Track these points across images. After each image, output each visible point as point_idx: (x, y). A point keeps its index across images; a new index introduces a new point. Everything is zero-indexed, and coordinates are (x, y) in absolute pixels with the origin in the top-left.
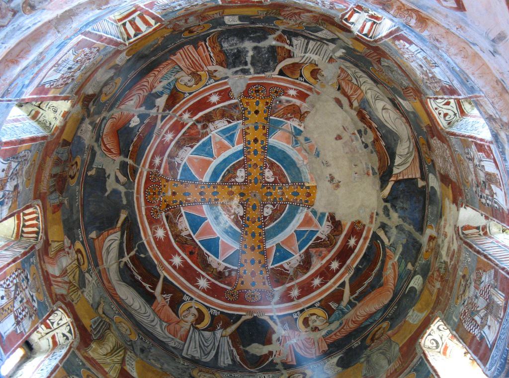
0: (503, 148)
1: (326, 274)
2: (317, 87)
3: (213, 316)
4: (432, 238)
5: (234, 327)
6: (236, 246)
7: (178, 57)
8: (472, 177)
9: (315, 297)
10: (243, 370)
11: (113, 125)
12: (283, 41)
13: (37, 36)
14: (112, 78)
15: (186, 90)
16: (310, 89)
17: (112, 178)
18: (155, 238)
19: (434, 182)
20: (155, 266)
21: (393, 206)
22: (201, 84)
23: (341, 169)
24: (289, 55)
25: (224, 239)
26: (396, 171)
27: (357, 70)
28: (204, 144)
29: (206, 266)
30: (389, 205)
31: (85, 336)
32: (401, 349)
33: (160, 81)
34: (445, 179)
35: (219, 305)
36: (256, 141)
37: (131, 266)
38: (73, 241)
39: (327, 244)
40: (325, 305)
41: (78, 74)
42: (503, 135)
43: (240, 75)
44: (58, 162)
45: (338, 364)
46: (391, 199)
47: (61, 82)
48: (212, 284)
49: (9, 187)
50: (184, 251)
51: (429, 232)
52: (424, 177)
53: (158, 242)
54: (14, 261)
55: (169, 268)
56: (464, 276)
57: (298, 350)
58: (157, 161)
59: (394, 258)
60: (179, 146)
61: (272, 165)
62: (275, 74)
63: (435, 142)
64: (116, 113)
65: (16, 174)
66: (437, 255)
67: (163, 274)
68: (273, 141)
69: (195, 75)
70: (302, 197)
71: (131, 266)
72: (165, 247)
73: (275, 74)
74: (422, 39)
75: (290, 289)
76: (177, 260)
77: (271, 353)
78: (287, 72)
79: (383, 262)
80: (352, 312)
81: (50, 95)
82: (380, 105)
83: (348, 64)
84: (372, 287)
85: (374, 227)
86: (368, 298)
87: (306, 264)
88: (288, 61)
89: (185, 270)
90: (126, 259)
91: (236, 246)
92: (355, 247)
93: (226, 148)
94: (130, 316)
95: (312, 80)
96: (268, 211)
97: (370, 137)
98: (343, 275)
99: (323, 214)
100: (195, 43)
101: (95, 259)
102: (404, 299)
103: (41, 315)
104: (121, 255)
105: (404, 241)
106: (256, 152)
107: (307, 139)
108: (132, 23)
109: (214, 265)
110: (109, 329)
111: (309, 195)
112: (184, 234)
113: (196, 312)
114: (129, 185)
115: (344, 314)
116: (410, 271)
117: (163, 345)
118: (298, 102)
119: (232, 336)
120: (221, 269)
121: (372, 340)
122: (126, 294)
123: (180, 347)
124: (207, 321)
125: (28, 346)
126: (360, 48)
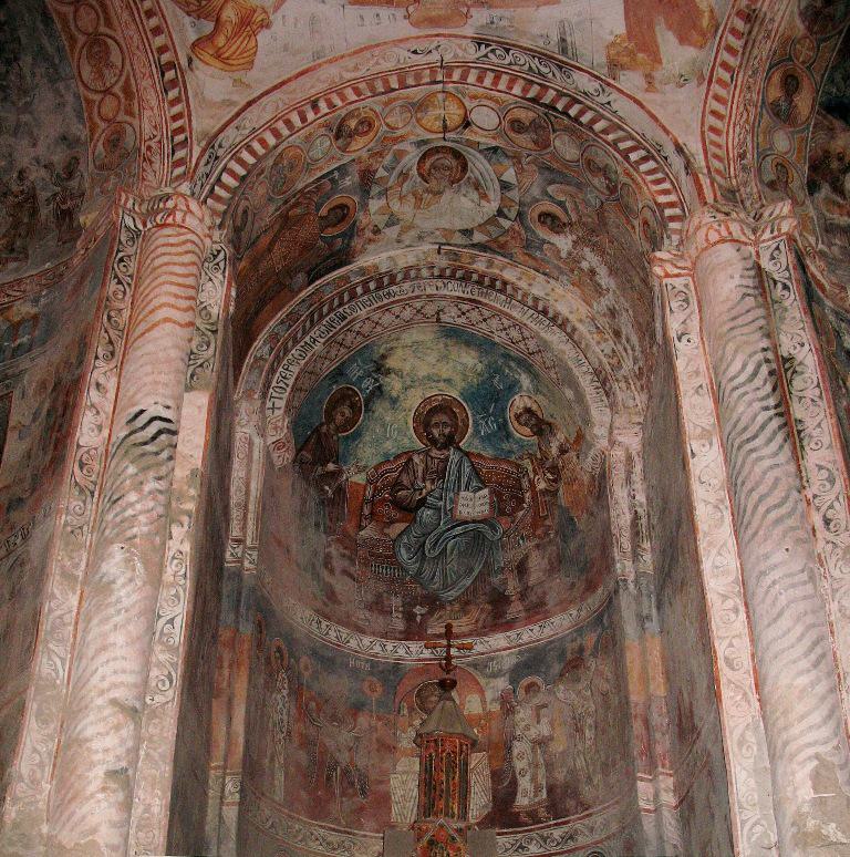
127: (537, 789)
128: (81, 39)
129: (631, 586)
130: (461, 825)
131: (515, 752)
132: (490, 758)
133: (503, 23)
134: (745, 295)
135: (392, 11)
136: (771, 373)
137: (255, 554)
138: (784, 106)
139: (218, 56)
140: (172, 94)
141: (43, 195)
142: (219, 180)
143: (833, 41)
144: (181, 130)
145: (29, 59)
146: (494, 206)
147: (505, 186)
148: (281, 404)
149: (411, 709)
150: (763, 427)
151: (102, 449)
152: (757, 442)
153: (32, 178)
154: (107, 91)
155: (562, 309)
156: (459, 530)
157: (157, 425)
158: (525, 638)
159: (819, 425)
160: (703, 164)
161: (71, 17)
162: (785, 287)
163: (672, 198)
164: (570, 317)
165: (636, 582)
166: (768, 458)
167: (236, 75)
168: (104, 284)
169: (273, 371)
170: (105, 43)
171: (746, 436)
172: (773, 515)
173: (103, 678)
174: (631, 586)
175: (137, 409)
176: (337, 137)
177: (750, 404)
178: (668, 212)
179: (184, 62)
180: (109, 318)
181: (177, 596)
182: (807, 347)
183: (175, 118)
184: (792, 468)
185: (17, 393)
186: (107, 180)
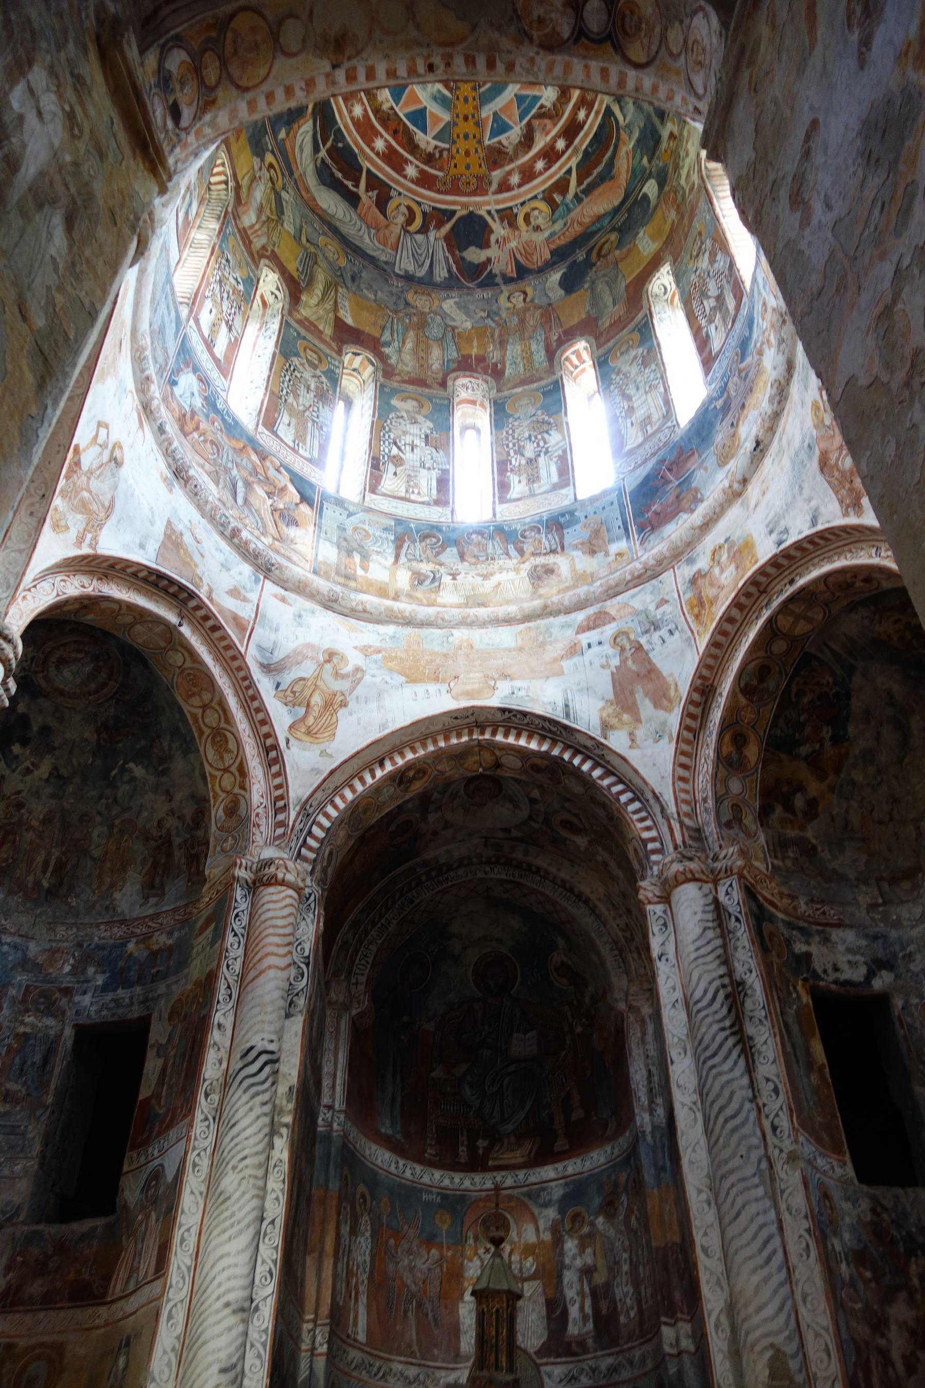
1: (550, 155)
3: (424, 214)
5: (448, 227)
6: (446, 117)
10: (461, 287)
18: (352, 119)
20: (355, 156)
25: (434, 109)
29: (413, 147)
31: (295, 289)
32: (627, 287)
35: (431, 199)
37: (329, 161)
39: (551, 115)
48: (422, 172)
50: (387, 130)
53: (356, 123)
55: (370, 159)
57: (518, 256)
59: (628, 145)
67: (366, 164)
71: (329, 161)
72: (366, 130)
75: (509, 173)
76: (380, 144)
77: (489, 260)
80: (578, 209)
86: (596, 193)
89: (392, 159)
90: (323, 153)
91: (446, 117)
92: (585, 122)
94: (335, 231)
98: (569, 159)
101: (288, 166)
104: (316, 149)
105: (642, 124)
109: (423, 145)
110: (316, 263)
112: (385, 107)
113: (406, 211)
115: (569, 210)
116: (644, 170)
117: (373, 260)
119: (447, 238)
120: (430, 149)
122: (329, 201)
123: (391, 260)
124: (418, 221)
127: (585, 1318)
129: (649, 1138)
130: (509, 1378)
131: (566, 1281)
132: (545, 1286)
133: (522, 693)
134: (705, 929)
135: (438, 686)
136: (727, 997)
137: (342, 1116)
138: (735, 757)
139: (309, 733)
141: (177, 841)
142: (310, 833)
144: (281, 797)
145: (168, 737)
146: (524, 813)
147: (533, 801)
148: (363, 979)
149: (476, 1238)
150: (720, 1047)
151: (222, 1080)
152: (717, 1060)
153: (168, 826)
154: (226, 770)
155: (586, 890)
156: (512, 1068)
157: (264, 1058)
158: (570, 1170)
159: (765, 1042)
160: (674, 809)
161: (200, 716)
162: (737, 920)
163: (653, 833)
164: (592, 897)
165: (652, 1132)
166: (731, 1070)
167: (322, 747)
168: (224, 939)
169: (356, 951)
171: (708, 1053)
172: (729, 1126)
173: (220, 1285)
174: (649, 1138)
175: (249, 1045)
176: (399, 785)
177: (711, 1025)
178: (650, 846)
179: (282, 744)
180: (228, 966)
181: (277, 1199)
182: (754, 973)
184: (745, 1081)
185: (155, 1015)
186: (226, 840)
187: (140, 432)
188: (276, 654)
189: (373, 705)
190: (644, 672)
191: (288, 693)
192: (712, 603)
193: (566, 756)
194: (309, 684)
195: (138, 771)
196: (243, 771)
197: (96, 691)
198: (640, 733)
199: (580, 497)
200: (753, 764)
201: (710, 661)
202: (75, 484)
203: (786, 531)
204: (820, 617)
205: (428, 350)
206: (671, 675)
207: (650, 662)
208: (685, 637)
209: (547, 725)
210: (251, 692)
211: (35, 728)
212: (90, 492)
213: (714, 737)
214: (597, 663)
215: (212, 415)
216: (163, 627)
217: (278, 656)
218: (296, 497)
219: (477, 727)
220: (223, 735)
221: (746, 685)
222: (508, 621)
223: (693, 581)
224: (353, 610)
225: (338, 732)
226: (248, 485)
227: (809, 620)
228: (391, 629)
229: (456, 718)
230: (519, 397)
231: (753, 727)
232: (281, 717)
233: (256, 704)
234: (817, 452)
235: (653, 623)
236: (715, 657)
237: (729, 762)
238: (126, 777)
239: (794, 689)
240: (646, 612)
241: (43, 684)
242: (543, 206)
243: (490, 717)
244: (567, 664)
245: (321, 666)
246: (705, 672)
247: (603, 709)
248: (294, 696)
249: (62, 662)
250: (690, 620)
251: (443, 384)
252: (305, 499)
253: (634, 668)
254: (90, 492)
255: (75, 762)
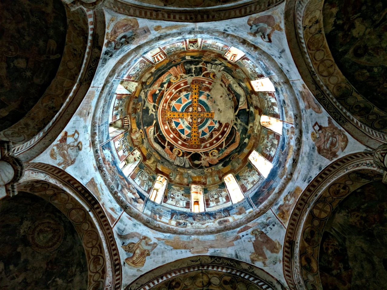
0: (279, 93)
1: (217, 139)
2: (215, 81)
3: (183, 153)
4: (251, 127)
5: (189, 156)
6: (189, 131)
7: (170, 71)
8: (266, 105)
9: (214, 146)
10: (193, 168)
11: (151, 93)
12: (204, 65)
13: (128, 55)
14: (150, 77)
15: (174, 82)
16: (213, 81)
17: (151, 110)
19: (252, 109)
20: (165, 138)
21: (239, 118)
22: (178, 80)
23: (222, 106)
24: (206, 70)
25: (186, 129)
26: (239, 106)
27: (228, 74)
28: (179, 100)
29: (181, 137)
30: (237, 117)
32: (242, 160)
33: (164, 78)
34: (256, 108)
35: (185, 149)
36: (195, 98)
37: (157, 137)
38: (139, 128)
39: (218, 130)
40: (217, 149)
41: (140, 73)
42: (279, 88)
43: (190, 77)
44: (134, 104)
45: (222, 166)
46: (238, 116)
47: (135, 75)
48: (183, 143)
49: (120, 109)
51: (250, 125)
52: (249, 108)
53: (166, 130)
54: (122, 133)
55: (169, 138)
56: (263, 137)
58: (165, 105)
59: (238, 134)
60: (171, 100)
61: (200, 106)
62: (201, 76)
63: (253, 96)
64: (151, 89)
65: (121, 106)
66: (253, 131)
67: (167, 140)
68: (201, 98)
69: (176, 77)
70: (210, 116)
71: (157, 137)
73: (201, 76)
74: (253, 57)
76: (172, 136)
77: (201, 163)
78: (205, 76)
79: (235, 135)
81: (132, 79)
82: (235, 85)
83: (225, 72)
84: (232, 143)
85: (232, 124)
86: (230, 146)
87: (211, 136)
88: (206, 72)
89: (174, 139)
90: (156, 135)
91: (189, 131)
93: (186, 101)
94: (158, 153)
95: (213, 78)
96: (199, 120)
97: (231, 96)
99: (216, 121)
100: (176, 66)
102: (242, 146)
103: (131, 150)
104: (154, 134)
106: (195, 102)
107: (211, 98)
108: (157, 57)
109: (183, 137)
111: (212, 115)
114: (156, 112)
115: (223, 151)
117: (168, 161)
118: (208, 85)
119: (189, 158)
120: (185, 138)
121: (233, 158)
122: (156, 146)
124: (181, 154)
125: (127, 160)
126: (230, 66)
128: (92, 257)
133: (218, 252)
135: (185, 250)
139: (133, 263)
140: (117, 273)
143: (317, 248)
145: (76, 266)
154: (97, 272)
170: (99, 259)
179: (122, 263)
183: (117, 280)
187: (89, 148)
188: (124, 232)
189: (160, 256)
190: (265, 241)
191: (127, 247)
192: (287, 211)
193: (238, 274)
194: (135, 245)
195: (60, 281)
196: (104, 271)
197: (51, 246)
198: (267, 262)
199: (233, 203)
200: (316, 270)
201: (290, 231)
202: (63, 146)
203: (311, 177)
204: (329, 210)
205: (183, 179)
206: (276, 240)
207: (267, 237)
208: (279, 225)
209: (229, 262)
210: (112, 243)
211: (22, 260)
212: (67, 153)
213: (298, 258)
214: (247, 240)
215: (114, 166)
216: (83, 212)
217: (125, 233)
218: (139, 197)
219: (201, 266)
220: (98, 259)
221: (307, 238)
222: (212, 233)
223: (279, 209)
224: (155, 227)
225: (145, 264)
226: (122, 187)
227: (326, 212)
228: (168, 235)
229: (193, 261)
230: (212, 187)
231: (312, 255)
232: (123, 255)
233: (114, 247)
234: (316, 148)
235: (266, 225)
236: (292, 229)
237: (306, 268)
238: (54, 284)
239: (324, 247)
240: (263, 223)
241: (30, 240)
242: (216, 151)
243: (206, 261)
244: (235, 243)
245: (141, 240)
246: (289, 235)
247: (251, 256)
248: (129, 249)
249: (41, 231)
250: (280, 220)
251: (188, 185)
252: (141, 198)
253: (261, 240)
254: (67, 153)
255: (34, 276)
